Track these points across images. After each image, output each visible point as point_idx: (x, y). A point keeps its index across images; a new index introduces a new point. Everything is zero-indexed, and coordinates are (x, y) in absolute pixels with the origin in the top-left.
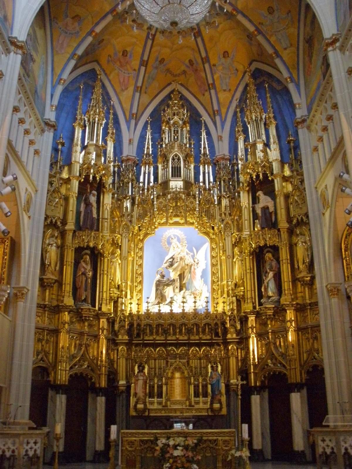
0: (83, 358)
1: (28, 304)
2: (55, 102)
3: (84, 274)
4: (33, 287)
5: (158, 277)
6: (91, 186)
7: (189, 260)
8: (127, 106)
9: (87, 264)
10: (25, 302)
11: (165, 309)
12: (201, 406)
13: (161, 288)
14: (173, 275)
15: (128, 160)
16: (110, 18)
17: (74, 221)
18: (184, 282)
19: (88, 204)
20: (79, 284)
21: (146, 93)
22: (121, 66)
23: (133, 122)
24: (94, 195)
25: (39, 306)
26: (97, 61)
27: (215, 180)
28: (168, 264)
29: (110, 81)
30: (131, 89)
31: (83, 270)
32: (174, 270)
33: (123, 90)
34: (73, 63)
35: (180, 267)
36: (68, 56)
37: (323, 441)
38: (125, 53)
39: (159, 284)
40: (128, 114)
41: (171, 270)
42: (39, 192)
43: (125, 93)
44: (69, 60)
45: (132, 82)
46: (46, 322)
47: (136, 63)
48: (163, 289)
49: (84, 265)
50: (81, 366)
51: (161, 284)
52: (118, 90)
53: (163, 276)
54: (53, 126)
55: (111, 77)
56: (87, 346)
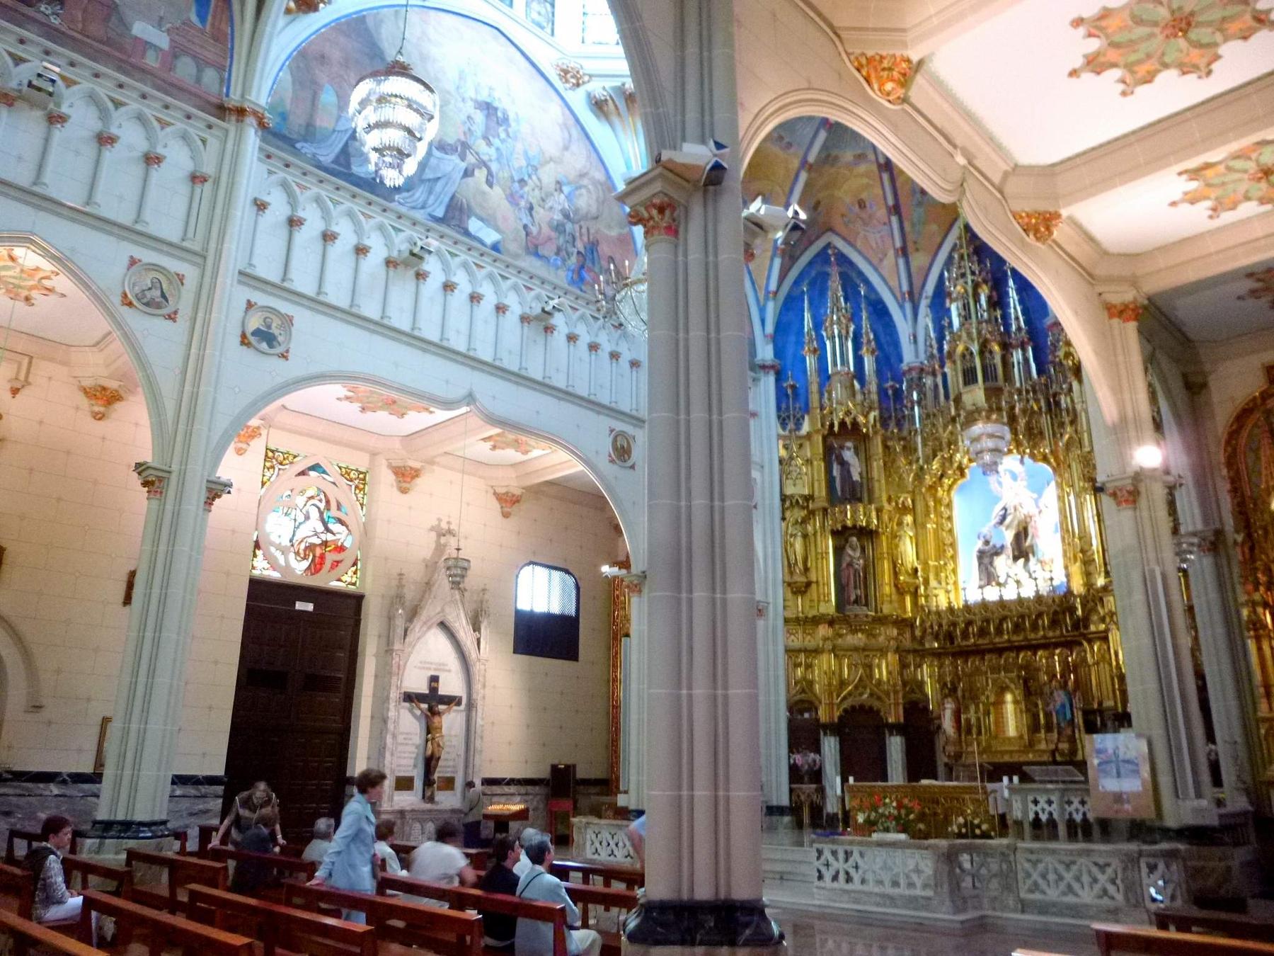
0: (861, 684)
1: (771, 622)
2: (770, 328)
3: (850, 565)
4: (775, 598)
5: (979, 544)
6: (843, 434)
7: (1028, 508)
8: (894, 284)
9: (854, 550)
10: (767, 620)
11: (992, 594)
12: (1043, 746)
13: (986, 560)
14: (1008, 536)
15: (910, 369)
16: (803, 176)
17: (824, 493)
18: (1028, 543)
19: (844, 464)
20: (844, 581)
21: (917, 250)
22: (865, 224)
23: (908, 306)
24: (849, 449)
25: (787, 621)
26: (831, 230)
27: (1039, 372)
28: (997, 520)
29: (860, 253)
30: (891, 253)
31: (848, 559)
32: (1007, 528)
33: (881, 260)
34: (777, 262)
35: (1016, 522)
36: (769, 254)
37: (1036, 802)
38: (862, 204)
39: (981, 555)
40: (898, 295)
41: (1003, 528)
42: (766, 469)
43: (885, 262)
44: (772, 260)
45: (888, 241)
46: (797, 641)
47: (881, 213)
48: (991, 563)
49: (850, 552)
50: (861, 694)
51: (986, 557)
52: (875, 261)
53: (987, 543)
54: (772, 367)
55: (859, 244)
56: (869, 667)
